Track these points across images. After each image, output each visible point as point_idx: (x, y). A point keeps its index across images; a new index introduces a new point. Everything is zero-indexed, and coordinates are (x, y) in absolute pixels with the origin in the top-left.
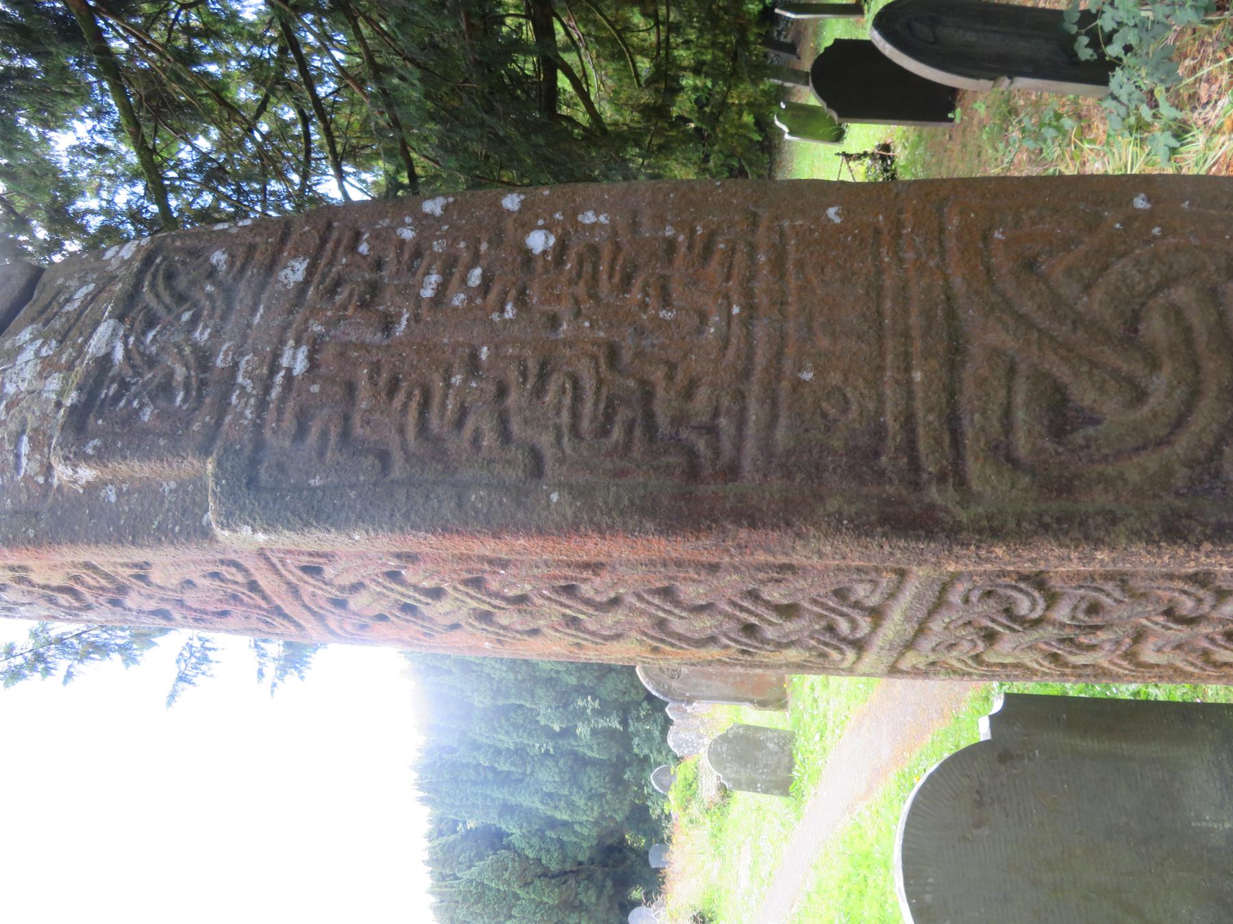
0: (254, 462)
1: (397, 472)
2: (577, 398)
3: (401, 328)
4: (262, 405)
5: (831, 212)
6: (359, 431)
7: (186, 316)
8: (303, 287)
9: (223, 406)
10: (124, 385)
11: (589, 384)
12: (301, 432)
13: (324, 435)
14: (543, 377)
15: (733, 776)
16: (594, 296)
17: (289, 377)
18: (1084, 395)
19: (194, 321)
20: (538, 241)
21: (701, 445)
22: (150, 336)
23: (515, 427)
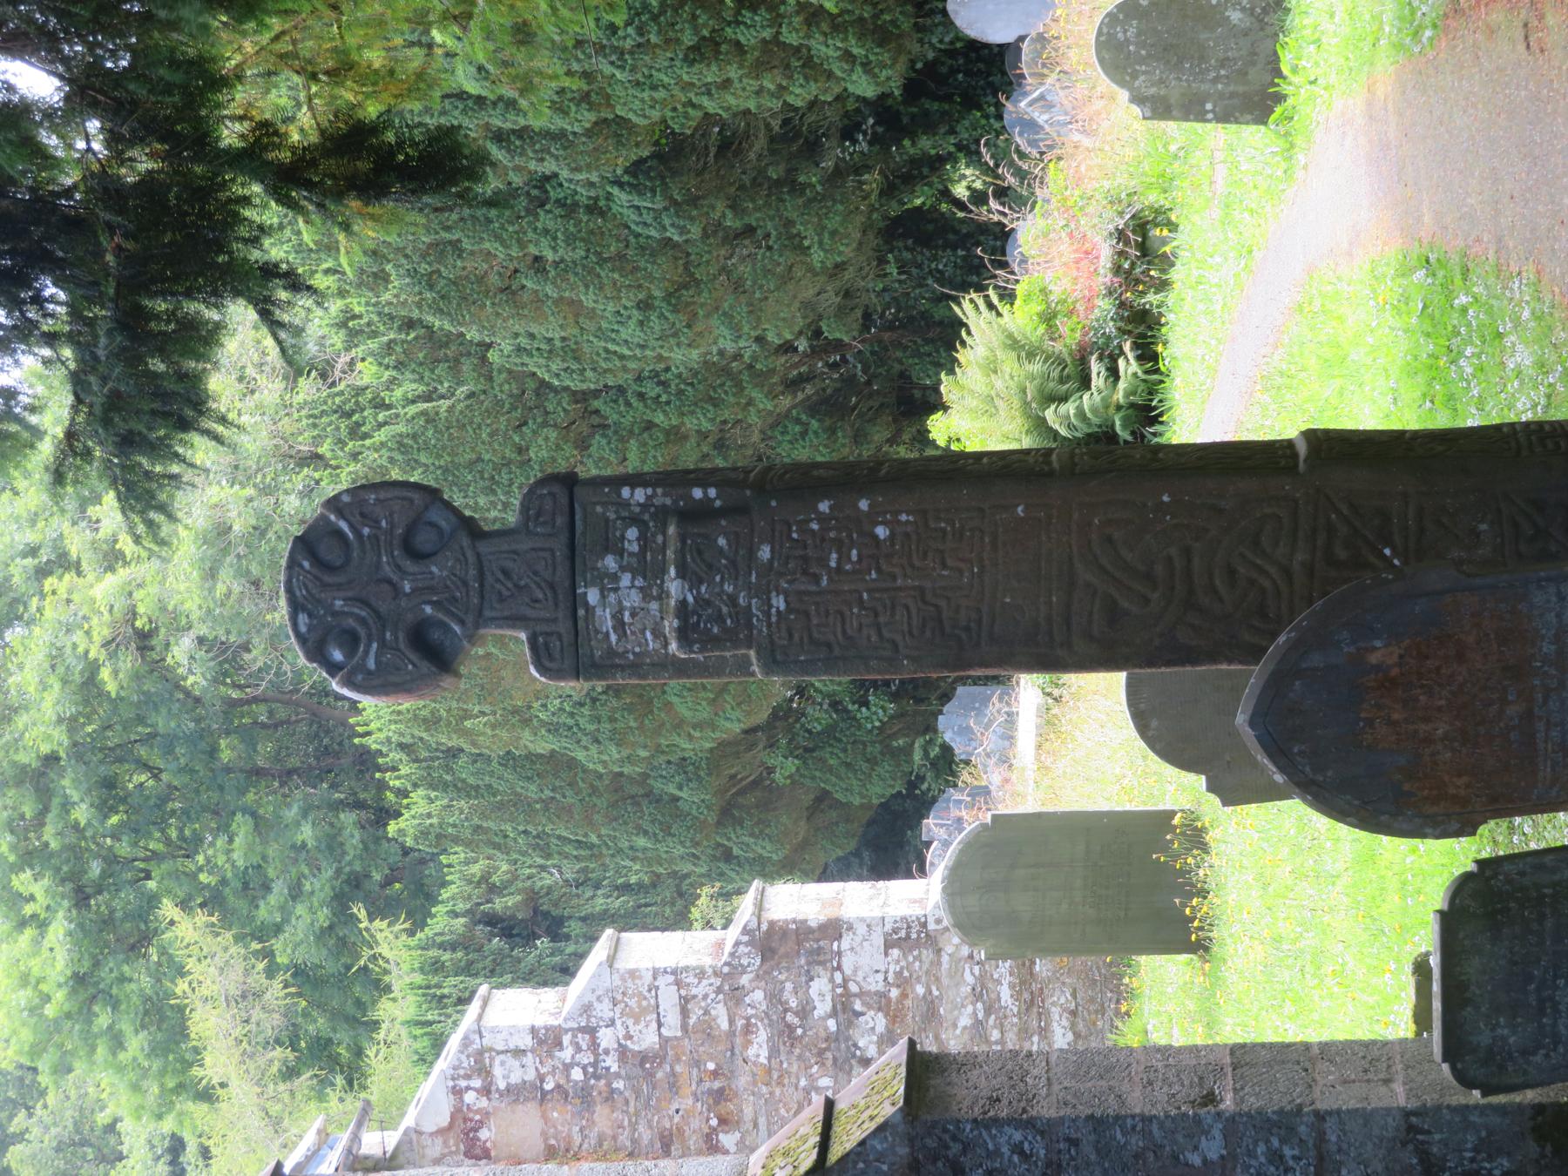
0: (773, 651)
1: (837, 651)
2: (909, 617)
3: (824, 582)
4: (769, 625)
5: (1020, 509)
6: (816, 635)
7: (718, 578)
8: (771, 561)
9: (750, 626)
10: (700, 616)
11: (914, 611)
12: (791, 636)
13: (801, 639)
14: (893, 607)
15: (1153, 90)
16: (912, 566)
17: (778, 611)
18: (1124, 604)
19: (722, 579)
20: (881, 532)
21: (964, 636)
22: (703, 589)
23: (886, 634)
